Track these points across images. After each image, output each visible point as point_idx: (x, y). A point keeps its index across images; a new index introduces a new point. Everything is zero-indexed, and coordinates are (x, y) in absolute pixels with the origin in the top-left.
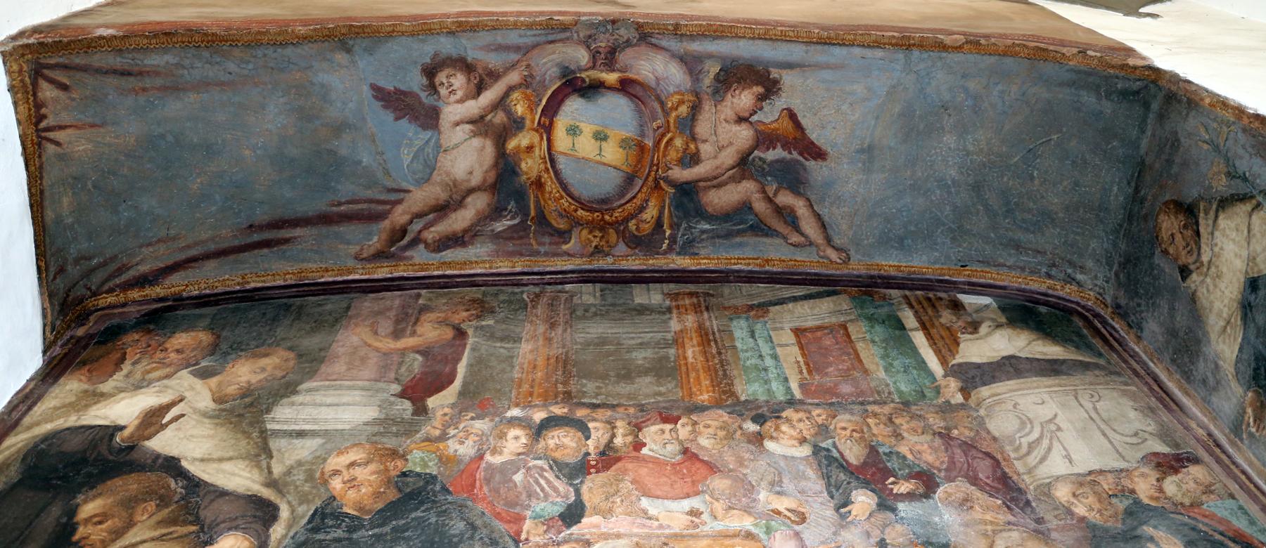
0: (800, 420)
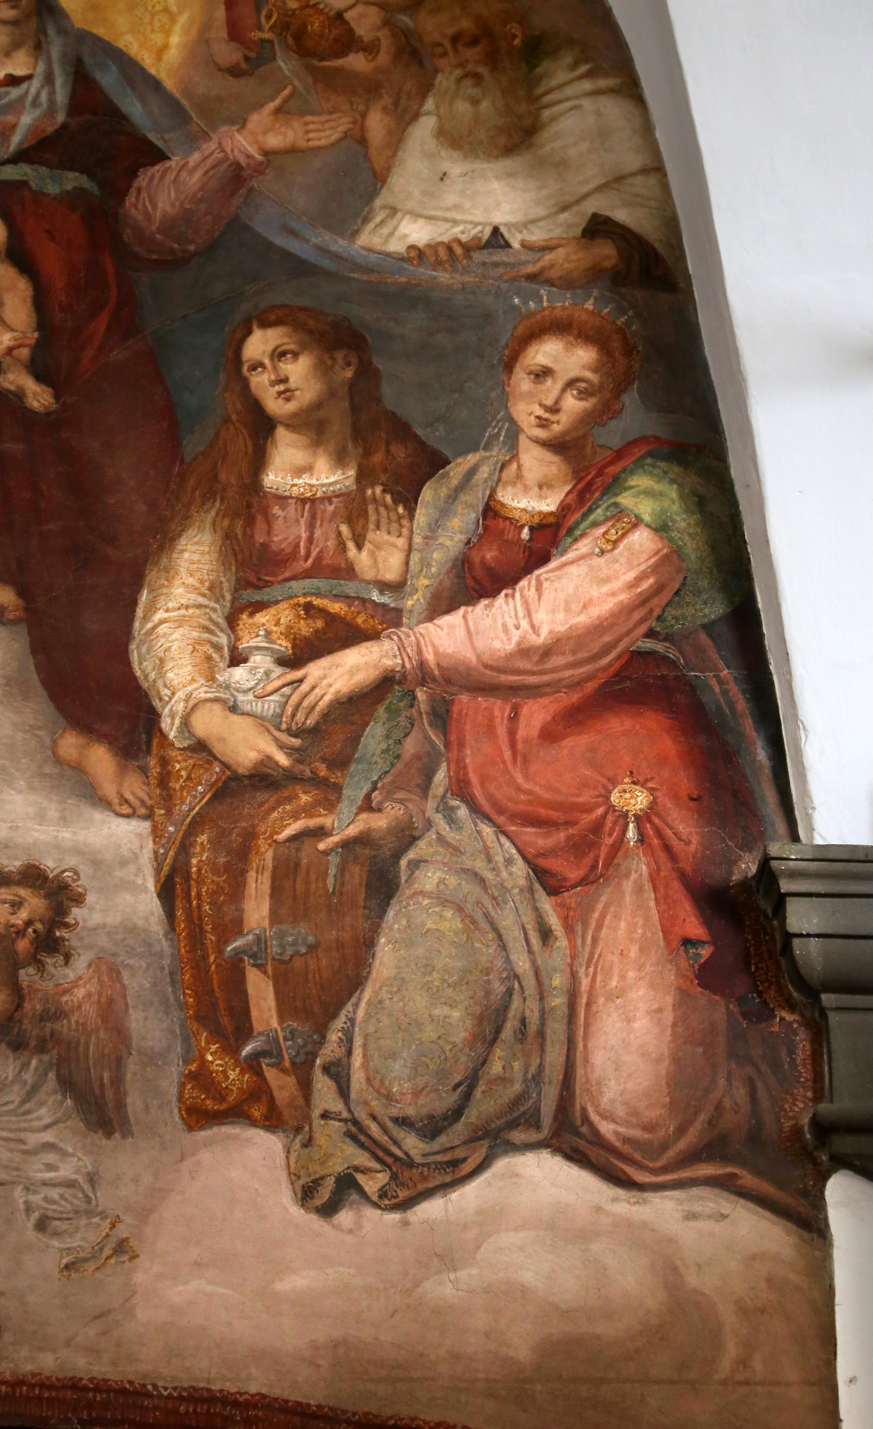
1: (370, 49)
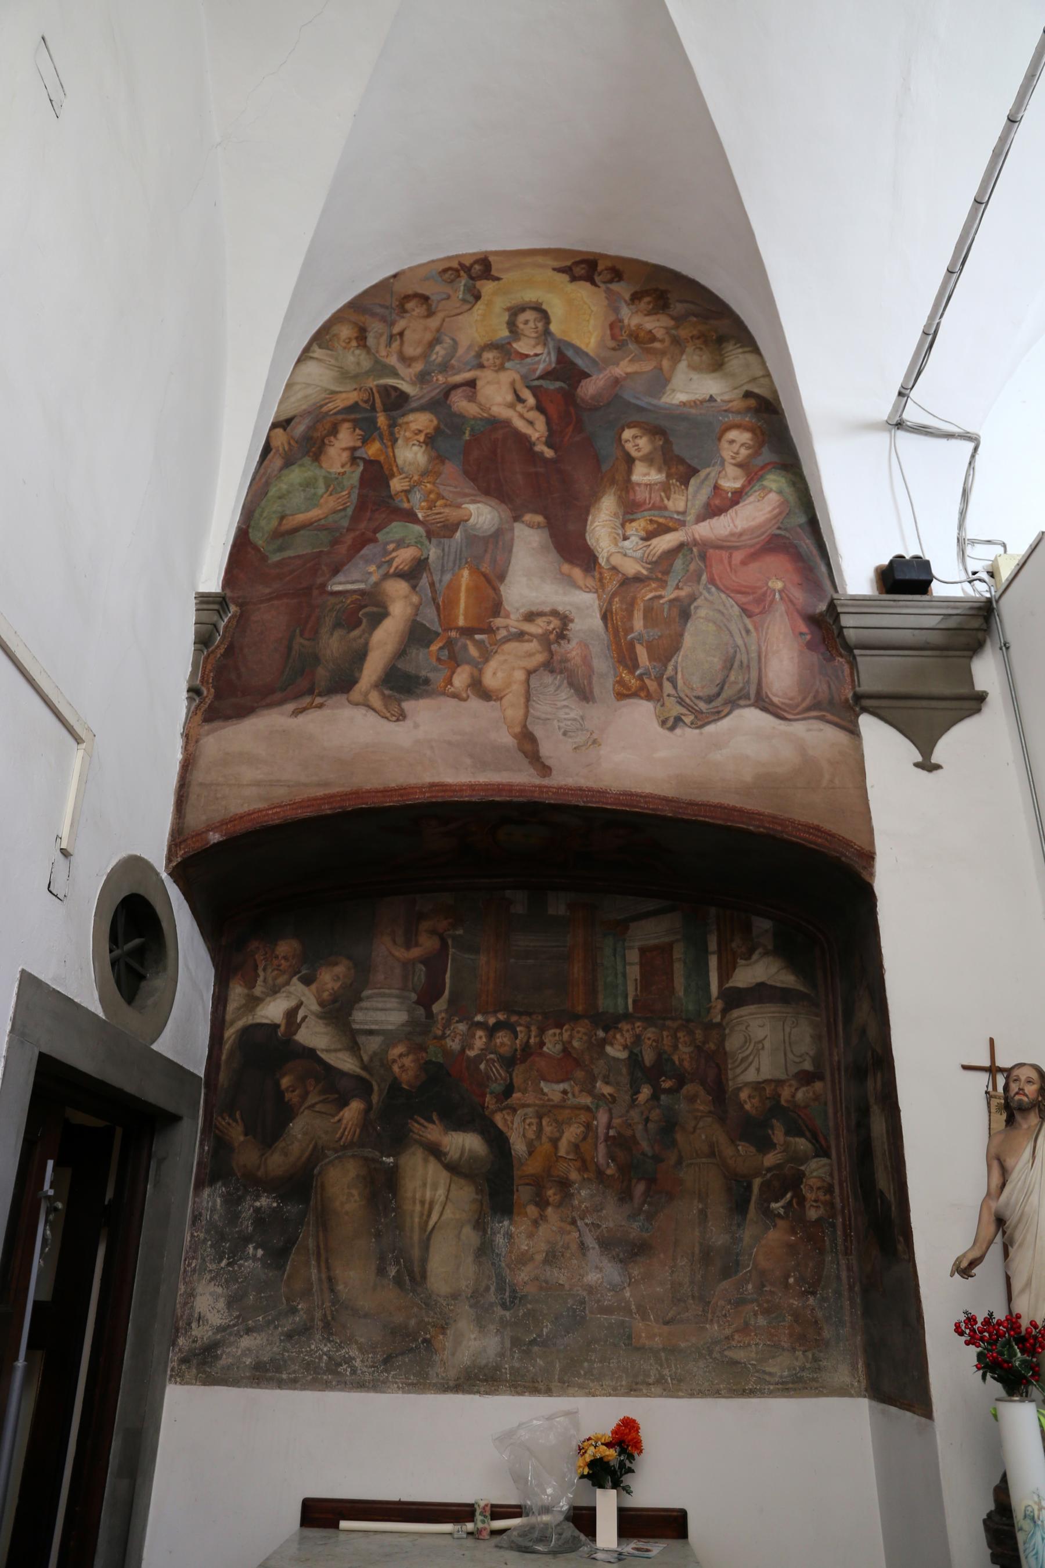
0: (628, 1031)
1: (662, 341)
